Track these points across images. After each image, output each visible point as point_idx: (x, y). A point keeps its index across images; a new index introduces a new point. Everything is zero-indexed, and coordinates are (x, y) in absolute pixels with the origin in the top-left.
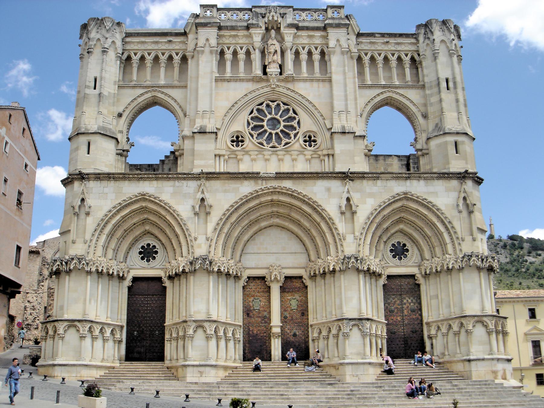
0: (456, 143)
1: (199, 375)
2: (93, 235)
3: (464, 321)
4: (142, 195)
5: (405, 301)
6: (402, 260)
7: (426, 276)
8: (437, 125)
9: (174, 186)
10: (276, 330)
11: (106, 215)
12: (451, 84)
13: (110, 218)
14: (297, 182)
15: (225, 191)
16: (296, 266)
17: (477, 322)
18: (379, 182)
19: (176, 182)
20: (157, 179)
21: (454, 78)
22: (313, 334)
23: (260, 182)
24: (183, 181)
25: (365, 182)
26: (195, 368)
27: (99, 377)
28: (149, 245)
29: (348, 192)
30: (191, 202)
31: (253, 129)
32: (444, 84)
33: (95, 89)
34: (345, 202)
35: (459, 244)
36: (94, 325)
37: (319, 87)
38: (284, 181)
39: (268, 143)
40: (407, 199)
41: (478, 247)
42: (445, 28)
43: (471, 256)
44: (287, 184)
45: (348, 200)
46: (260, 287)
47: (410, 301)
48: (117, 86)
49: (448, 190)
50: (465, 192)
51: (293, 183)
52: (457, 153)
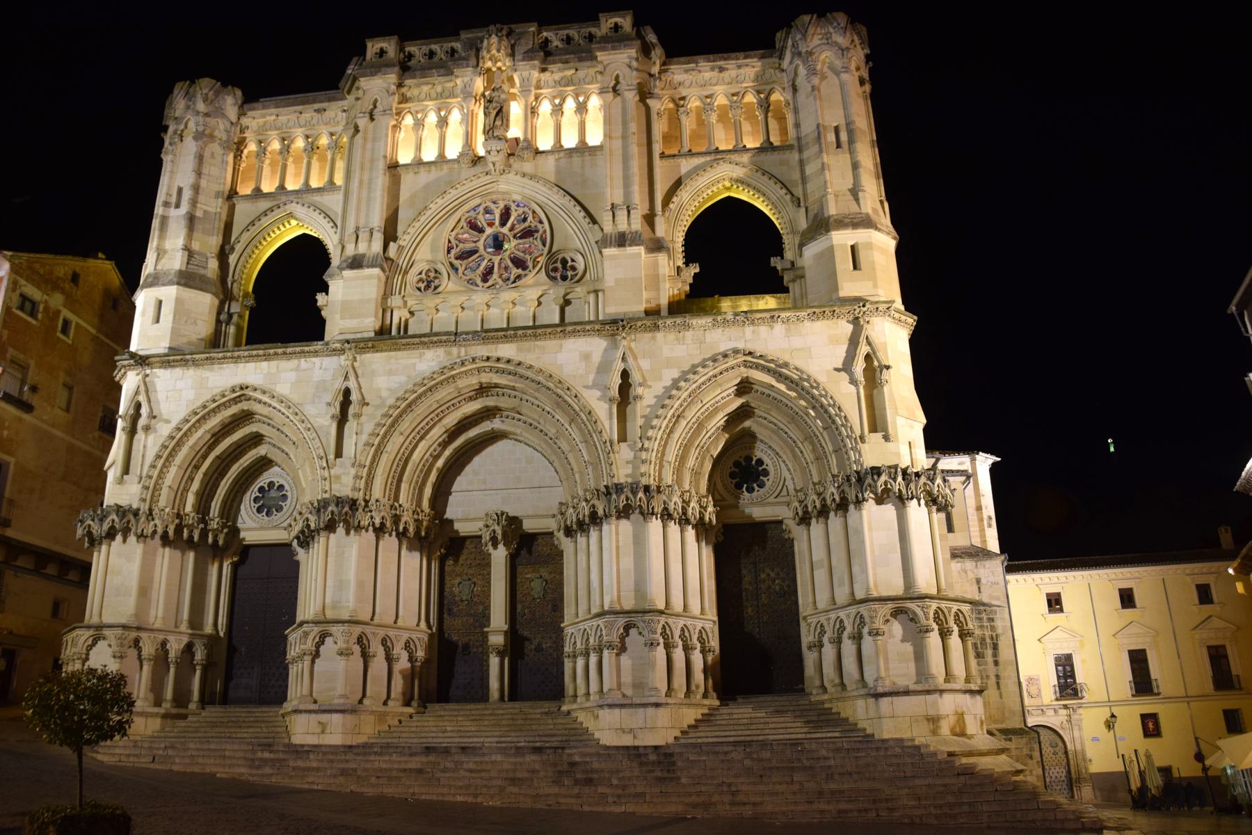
0: (853, 247)
1: (319, 730)
2: (153, 466)
3: (863, 609)
4: (242, 388)
5: (763, 576)
6: (755, 493)
7: (805, 520)
8: (816, 216)
9: (297, 369)
10: (497, 640)
11: (179, 429)
12: (844, 137)
13: (185, 434)
14: (526, 344)
15: (390, 373)
16: (541, 513)
17: (896, 613)
18: (689, 334)
19: (304, 363)
20: (267, 358)
21: (849, 124)
22: (568, 649)
23: (455, 350)
24: (314, 359)
25: (659, 335)
26: (313, 716)
27: (149, 733)
28: (271, 484)
29: (624, 359)
30: (329, 398)
31: (457, 258)
32: (831, 137)
33: (178, 206)
34: (617, 381)
35: (854, 449)
36: (144, 635)
37: (583, 167)
38: (500, 346)
39: (485, 280)
40: (746, 364)
41: (898, 454)
42: (831, 30)
43: (879, 475)
44: (507, 350)
45: (625, 375)
46: (472, 556)
47: (772, 575)
48: (220, 200)
49: (834, 341)
50: (869, 343)
51: (519, 350)
52: (855, 267)
